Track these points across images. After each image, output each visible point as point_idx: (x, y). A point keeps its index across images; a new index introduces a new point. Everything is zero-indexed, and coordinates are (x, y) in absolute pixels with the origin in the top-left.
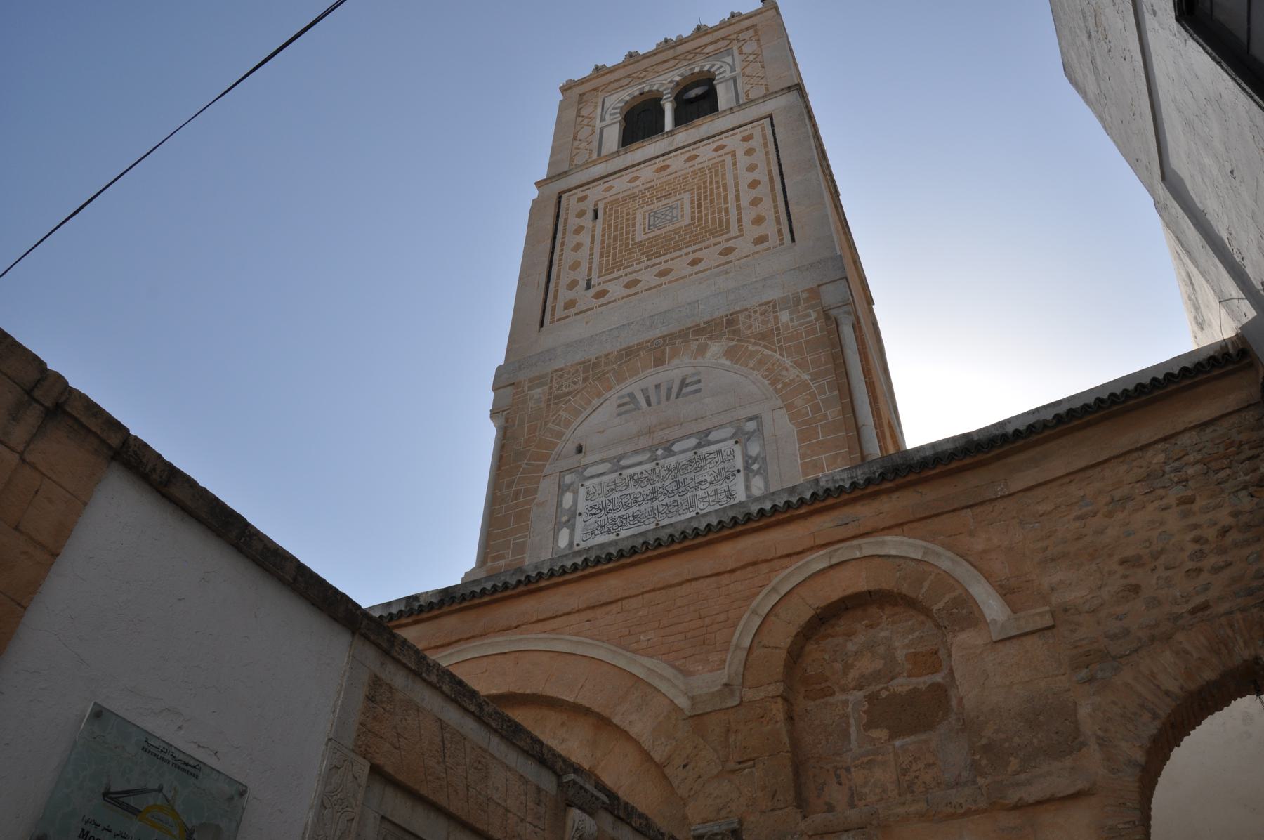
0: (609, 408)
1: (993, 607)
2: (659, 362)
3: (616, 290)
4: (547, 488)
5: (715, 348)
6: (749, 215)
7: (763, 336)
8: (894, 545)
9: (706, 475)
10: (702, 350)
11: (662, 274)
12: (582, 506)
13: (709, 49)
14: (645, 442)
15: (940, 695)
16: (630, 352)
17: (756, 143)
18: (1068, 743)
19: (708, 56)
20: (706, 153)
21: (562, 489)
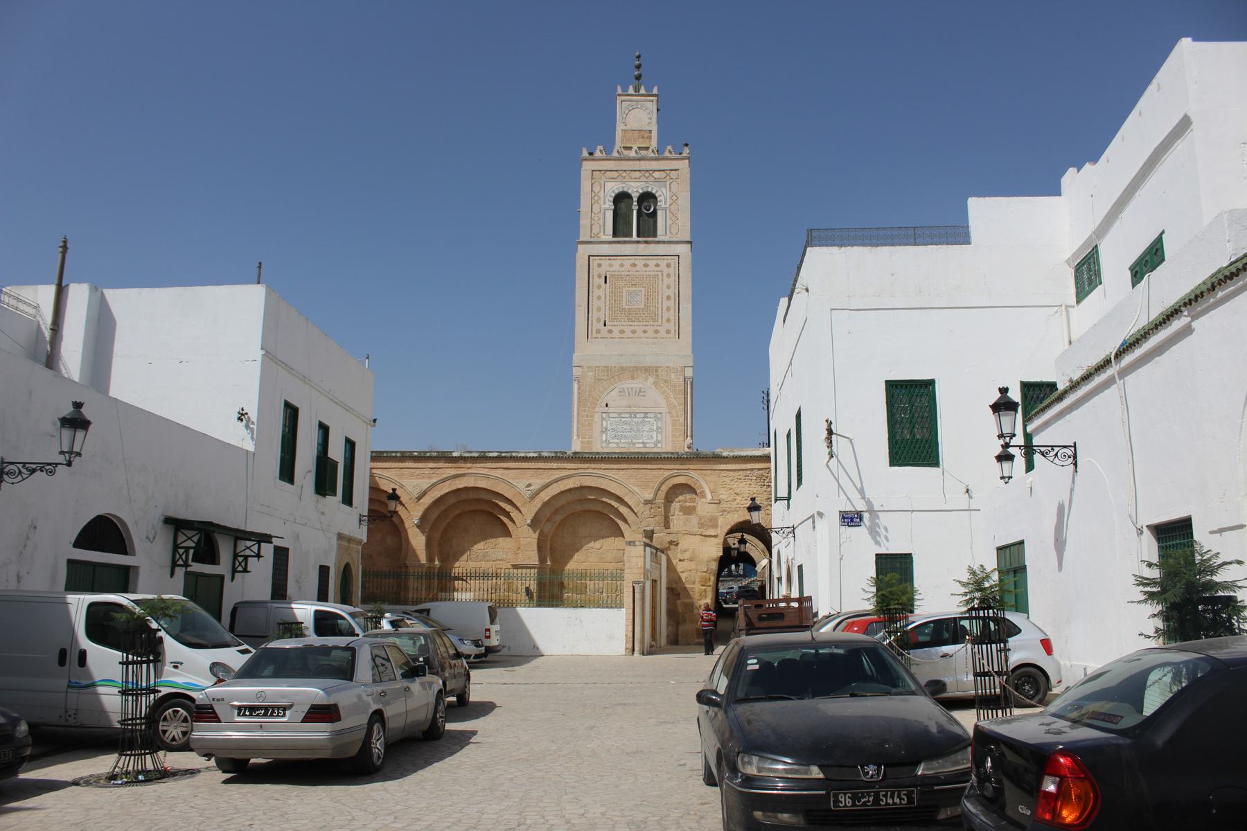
0: (616, 391)
1: (709, 496)
2: (633, 378)
3: (616, 330)
4: (597, 417)
5: (651, 380)
6: (665, 318)
7: (666, 381)
8: (693, 474)
9: (646, 428)
10: (646, 379)
11: (634, 332)
12: (609, 428)
13: (656, 175)
14: (628, 410)
15: (694, 508)
16: (623, 369)
17: (671, 271)
18: (715, 526)
19: (656, 180)
20: (652, 263)
21: (603, 419)
